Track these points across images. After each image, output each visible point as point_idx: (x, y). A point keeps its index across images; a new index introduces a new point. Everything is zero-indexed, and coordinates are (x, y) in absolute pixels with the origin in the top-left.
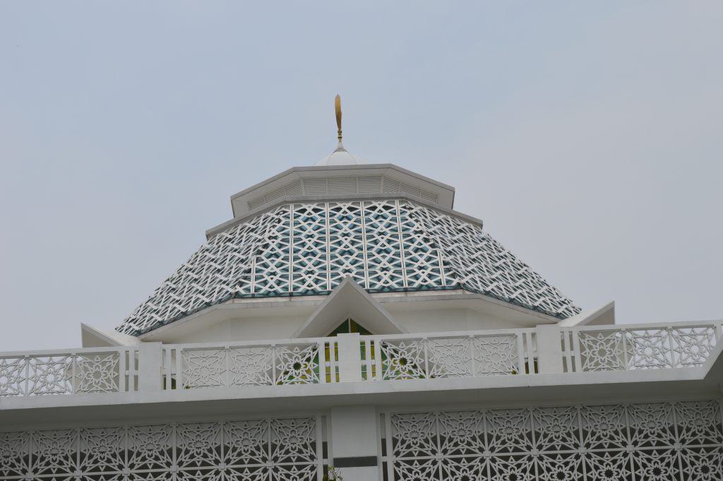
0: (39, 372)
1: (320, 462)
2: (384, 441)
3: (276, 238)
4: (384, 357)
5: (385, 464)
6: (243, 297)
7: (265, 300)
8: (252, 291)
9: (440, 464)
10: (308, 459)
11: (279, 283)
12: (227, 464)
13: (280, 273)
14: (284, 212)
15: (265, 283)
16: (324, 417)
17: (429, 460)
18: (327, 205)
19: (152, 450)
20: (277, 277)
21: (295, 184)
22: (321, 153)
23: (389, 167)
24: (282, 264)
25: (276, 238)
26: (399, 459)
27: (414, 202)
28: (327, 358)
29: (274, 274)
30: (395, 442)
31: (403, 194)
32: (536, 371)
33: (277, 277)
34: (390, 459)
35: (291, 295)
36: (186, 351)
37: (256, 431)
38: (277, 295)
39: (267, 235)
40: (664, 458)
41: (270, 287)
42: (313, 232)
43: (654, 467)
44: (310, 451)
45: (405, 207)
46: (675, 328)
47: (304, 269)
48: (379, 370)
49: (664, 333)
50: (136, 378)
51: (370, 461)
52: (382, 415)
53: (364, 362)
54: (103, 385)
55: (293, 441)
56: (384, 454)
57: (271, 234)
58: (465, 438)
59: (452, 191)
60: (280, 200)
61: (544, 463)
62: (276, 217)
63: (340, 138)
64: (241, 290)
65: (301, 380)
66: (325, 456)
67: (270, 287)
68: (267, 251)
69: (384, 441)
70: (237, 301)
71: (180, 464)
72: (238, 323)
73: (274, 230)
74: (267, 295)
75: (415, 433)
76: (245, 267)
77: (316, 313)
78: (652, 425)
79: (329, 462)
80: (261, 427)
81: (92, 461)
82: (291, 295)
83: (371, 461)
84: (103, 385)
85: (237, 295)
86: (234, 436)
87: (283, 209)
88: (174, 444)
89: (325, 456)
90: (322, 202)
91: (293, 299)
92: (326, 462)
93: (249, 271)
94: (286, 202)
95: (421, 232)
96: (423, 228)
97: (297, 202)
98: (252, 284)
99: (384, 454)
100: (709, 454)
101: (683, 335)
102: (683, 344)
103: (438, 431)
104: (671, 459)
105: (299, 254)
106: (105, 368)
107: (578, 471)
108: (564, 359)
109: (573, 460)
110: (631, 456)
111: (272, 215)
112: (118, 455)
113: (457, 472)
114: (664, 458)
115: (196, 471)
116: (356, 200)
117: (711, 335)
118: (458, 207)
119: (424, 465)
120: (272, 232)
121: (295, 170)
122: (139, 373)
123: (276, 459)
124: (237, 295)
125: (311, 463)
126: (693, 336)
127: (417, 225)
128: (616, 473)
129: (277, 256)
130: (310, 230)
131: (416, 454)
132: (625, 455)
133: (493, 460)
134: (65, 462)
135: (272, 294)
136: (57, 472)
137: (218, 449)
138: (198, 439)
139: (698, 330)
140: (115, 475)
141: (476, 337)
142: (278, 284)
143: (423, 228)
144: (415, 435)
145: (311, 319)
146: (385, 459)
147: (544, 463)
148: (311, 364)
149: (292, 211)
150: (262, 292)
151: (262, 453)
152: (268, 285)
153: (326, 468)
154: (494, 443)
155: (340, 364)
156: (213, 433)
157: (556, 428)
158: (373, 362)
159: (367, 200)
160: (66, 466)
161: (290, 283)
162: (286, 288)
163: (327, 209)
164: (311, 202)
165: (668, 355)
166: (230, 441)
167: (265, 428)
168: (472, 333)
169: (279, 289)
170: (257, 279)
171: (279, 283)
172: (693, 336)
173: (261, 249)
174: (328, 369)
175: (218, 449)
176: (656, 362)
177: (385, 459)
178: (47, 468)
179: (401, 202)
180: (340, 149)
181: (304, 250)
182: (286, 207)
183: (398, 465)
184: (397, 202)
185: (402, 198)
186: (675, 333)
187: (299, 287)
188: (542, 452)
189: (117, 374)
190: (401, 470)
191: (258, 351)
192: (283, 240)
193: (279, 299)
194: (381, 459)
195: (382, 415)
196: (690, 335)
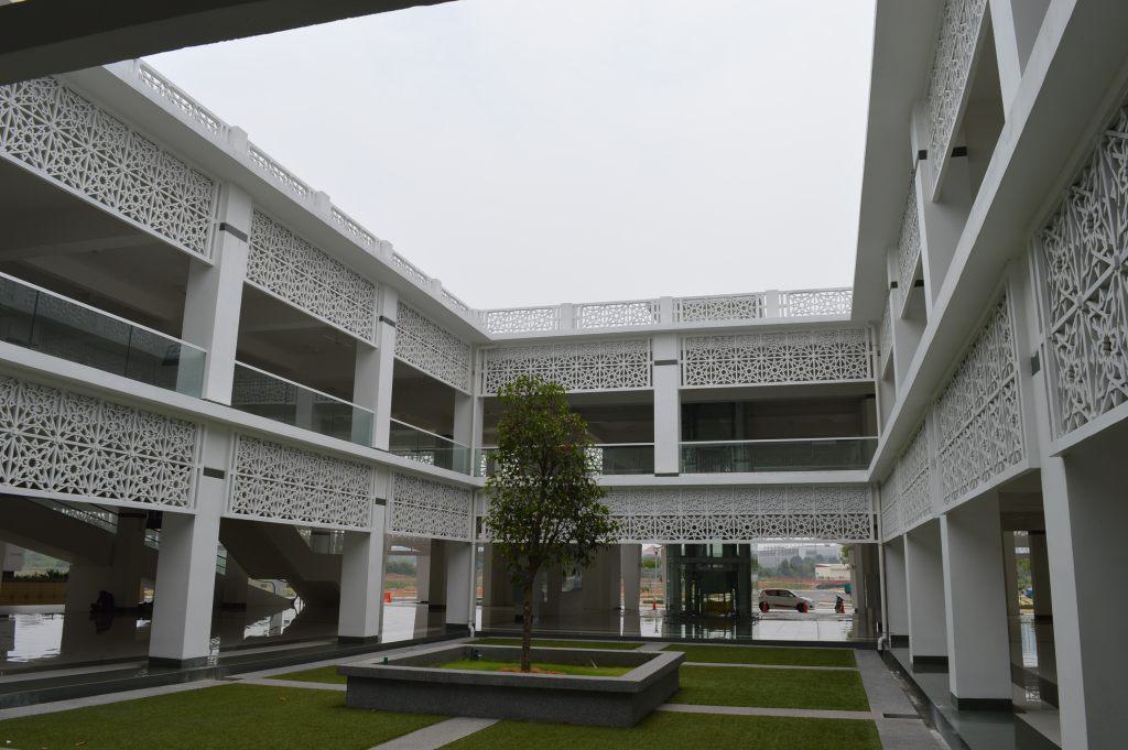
1: (649, 363)
32: (761, 316)
34: (685, 362)
48: (681, 316)
51: (674, 362)
52: (682, 339)
55: (639, 349)
83: (674, 362)
126: (827, 296)
139: (830, 293)
154: (715, 354)
165: (839, 306)
172: (827, 296)
194: (680, 362)
195: (682, 339)
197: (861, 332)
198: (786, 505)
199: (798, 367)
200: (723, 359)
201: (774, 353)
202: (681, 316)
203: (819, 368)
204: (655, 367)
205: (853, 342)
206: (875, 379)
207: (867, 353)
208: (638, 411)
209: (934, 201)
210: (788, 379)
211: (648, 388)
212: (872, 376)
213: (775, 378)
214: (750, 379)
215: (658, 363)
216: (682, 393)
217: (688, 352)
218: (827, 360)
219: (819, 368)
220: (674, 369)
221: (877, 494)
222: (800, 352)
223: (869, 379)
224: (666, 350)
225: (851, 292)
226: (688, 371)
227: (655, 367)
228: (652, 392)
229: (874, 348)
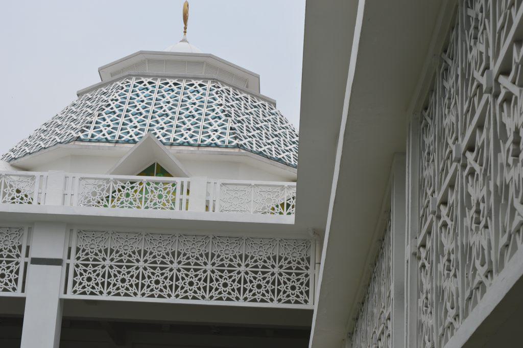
1: (22, 260)
2: (70, 249)
3: (117, 100)
5: (68, 265)
6: (82, 141)
7: (97, 144)
8: (227, 143)
11: (219, 138)
13: (220, 131)
14: (128, 82)
15: (209, 136)
18: (184, 81)
20: (191, 132)
21: (141, 64)
22: (172, 45)
23: (210, 56)
24: (223, 124)
25: (117, 100)
26: (79, 262)
27: (223, 83)
28: (182, 193)
29: (216, 131)
30: (78, 250)
31: (215, 76)
33: (191, 132)
34: (73, 262)
35: (199, 146)
36: (224, 184)
37: (101, 239)
38: (189, 145)
39: (111, 97)
41: (212, 140)
42: (196, 101)
44: (17, 251)
45: (214, 86)
47: (211, 128)
50: (187, 200)
51: (57, 262)
52: (71, 230)
53: (187, 197)
54: (131, 203)
57: (113, 97)
59: (258, 77)
60: (126, 73)
62: (121, 85)
63: (185, 32)
64: (81, 135)
66: (27, 256)
67: (212, 140)
68: (108, 109)
69: (70, 249)
70: (77, 143)
72: (76, 158)
73: (116, 95)
74: (209, 145)
75: (93, 245)
76: (89, 119)
77: (126, 157)
78: (261, 253)
79: (28, 260)
80: (272, 243)
82: (199, 146)
83: (58, 262)
84: (164, 204)
85: (78, 139)
86: (118, 242)
87: (128, 80)
89: (27, 256)
90: (156, 77)
91: (117, 145)
93: (91, 123)
94: (130, 75)
95: (221, 105)
96: (224, 102)
97: (138, 76)
98: (90, 132)
99: (69, 258)
103: (108, 246)
105: (209, 117)
106: (166, 192)
108: (208, 201)
111: (119, 83)
116: (181, 78)
118: (264, 92)
119: (96, 268)
120: (115, 96)
121: (141, 53)
123: (239, 265)
124: (78, 139)
127: (219, 99)
129: (220, 118)
130: (193, 99)
131: (192, 264)
133: (145, 269)
135: (213, 145)
137: (139, 252)
138: (126, 243)
141: (256, 185)
142: (164, 136)
143: (224, 102)
145: (122, 160)
146: (68, 261)
149: (133, 82)
150: (205, 143)
151: (272, 262)
152: (211, 138)
153: (26, 264)
155: (190, 197)
157: (193, 250)
159: (188, 79)
161: (199, 137)
162: (223, 142)
163: (209, 85)
164: (149, 76)
166: (115, 245)
167: (140, 239)
168: (253, 182)
169: (218, 142)
170: (203, 133)
171: (192, 136)
173: (103, 107)
174: (181, 200)
175: (139, 252)
177: (68, 261)
179: (213, 82)
180: (184, 40)
181: (213, 114)
182: (129, 79)
183: (77, 266)
184: (210, 82)
185: (214, 79)
187: (205, 141)
189: (174, 197)
191: (242, 188)
192: (199, 106)
193: (108, 144)
194: (66, 261)
200: (123, 263)
204: (31, 267)
210: (173, 295)
211: (18, 294)
214: (123, 291)
215: (36, 261)
216: (65, 305)
220: (58, 270)
222: (260, 263)
224: (46, 245)
226: (75, 275)
227: (31, 267)
228: (22, 301)
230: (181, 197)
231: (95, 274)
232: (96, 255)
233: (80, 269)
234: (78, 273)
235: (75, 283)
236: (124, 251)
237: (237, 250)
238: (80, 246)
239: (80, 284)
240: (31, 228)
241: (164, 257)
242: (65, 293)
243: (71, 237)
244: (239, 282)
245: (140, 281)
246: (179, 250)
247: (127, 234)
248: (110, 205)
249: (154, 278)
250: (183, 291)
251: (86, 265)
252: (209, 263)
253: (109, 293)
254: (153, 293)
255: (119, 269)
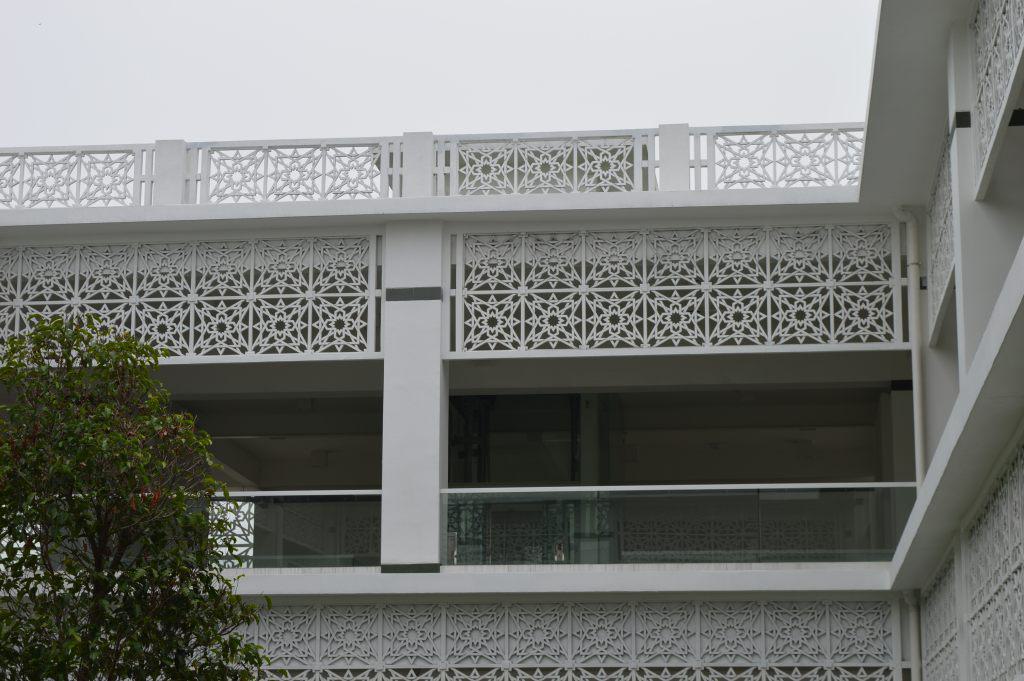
0: (37, 174)
1: (372, 293)
2: (453, 269)
4: (462, 164)
5: (453, 300)
9: (645, 297)
10: (239, 292)
12: (469, 289)
16: (379, 237)
17: (120, 304)
19: (50, 277)
26: (471, 292)
32: (645, 187)
34: (460, 293)
40: (351, 308)
43: (499, 319)
46: (844, 130)
48: (454, 179)
49: (829, 137)
51: (433, 293)
52: (454, 236)
56: (453, 286)
58: (741, 263)
61: (842, 297)
65: (550, 185)
66: (379, 286)
69: (453, 269)
71: (83, 295)
79: (382, 293)
81: (151, 284)
83: (433, 293)
88: (192, 266)
89: (379, 286)
92: (378, 293)
99: (453, 286)
100: (808, 296)
101: (791, 142)
102: (790, 153)
104: (299, 311)
107: (887, 307)
109: (473, 306)
110: (769, 295)
112: (301, 274)
113: (172, 319)
114: (351, 308)
115: (160, 303)
117: (829, 143)
119: (114, 311)
122: (404, 171)
125: (361, 294)
128: (873, 314)
132: (699, 294)
133: (591, 297)
134: (119, 285)
136: (167, 296)
139: (811, 136)
140: (120, 304)
144: (737, 256)
146: (453, 292)
147: (842, 297)
148: (624, 165)
153: (378, 300)
156: (183, 256)
158: (447, 170)
160: (120, 290)
172: (805, 143)
176: (814, 175)
177: (453, 292)
178: (97, 292)
183: (469, 300)
186: (843, 137)
188: (593, 290)
190: (203, 312)
194: (448, 292)
196: (801, 142)
197: (881, 231)
198: (695, 644)
199: (732, 310)
200: (554, 288)
201: (675, 276)
202: (454, 179)
203: (781, 316)
204: (386, 305)
205: (862, 253)
206: (913, 345)
207: (896, 283)
208: (349, 409)
209: (977, 200)
211: (370, 354)
212: (906, 338)
213: (676, 336)
214: (615, 338)
215: (395, 295)
216: (452, 369)
217: (468, 271)
218: (800, 297)
219: (781, 316)
220: (435, 309)
221: (912, 616)
223: (897, 344)
225: (861, 135)
227: (388, 307)
228: (378, 365)
229: (912, 271)
230: (390, 171)
231: (350, 314)
232: (684, 272)
233: (475, 306)
234: (472, 313)
235: (467, 329)
236: (734, 263)
237: (125, 269)
238: (592, 260)
239: (723, 325)
240: (456, 236)
241: (871, 268)
242: (453, 348)
243: (453, 246)
244: (517, 315)
245: (707, 317)
246: (198, 270)
247: (737, 231)
248: (575, 187)
249: (215, 321)
250: (850, 327)
251: (486, 298)
252: (193, 290)
253: (198, 351)
254: (794, 335)
255: (790, 295)
